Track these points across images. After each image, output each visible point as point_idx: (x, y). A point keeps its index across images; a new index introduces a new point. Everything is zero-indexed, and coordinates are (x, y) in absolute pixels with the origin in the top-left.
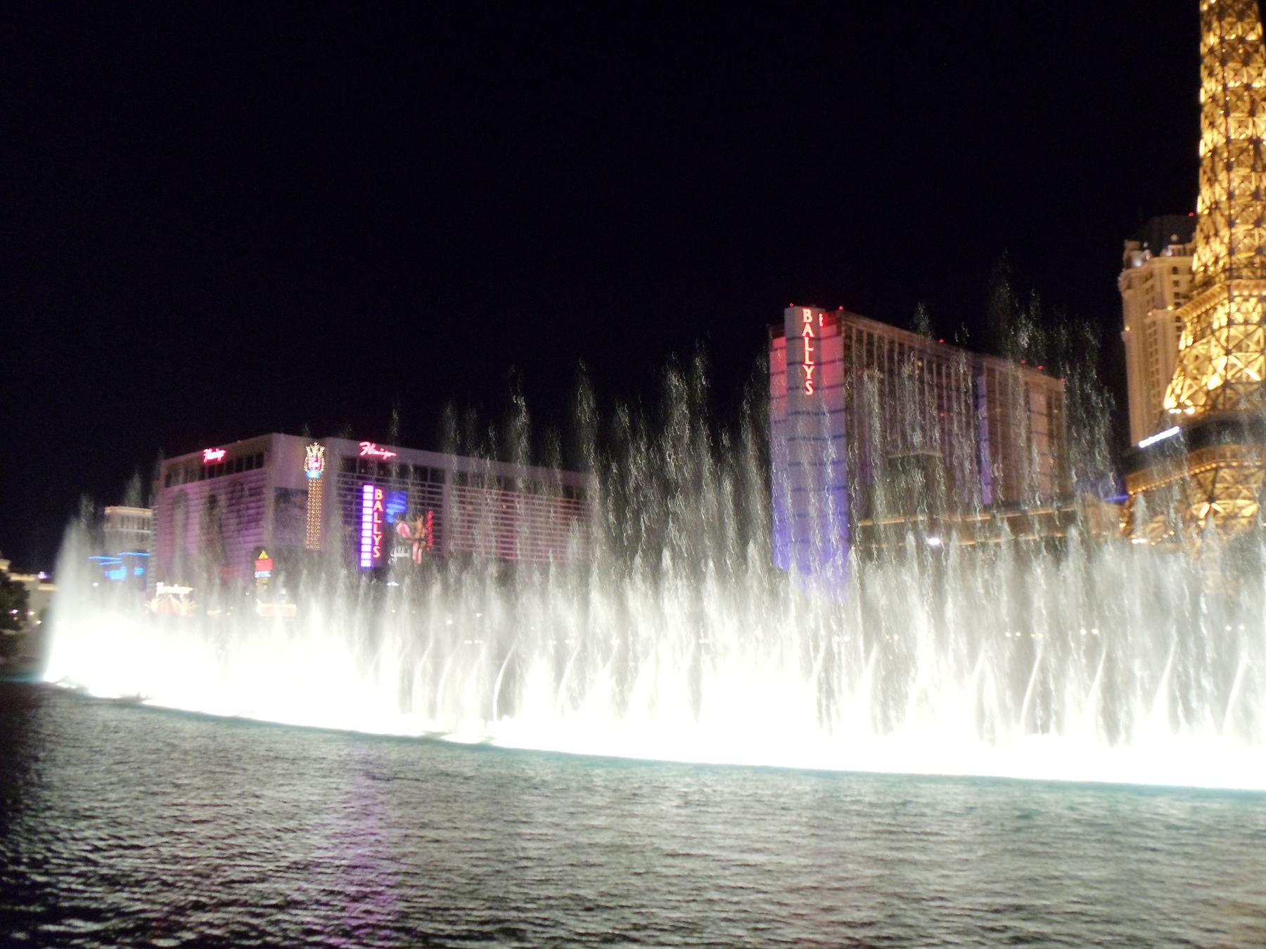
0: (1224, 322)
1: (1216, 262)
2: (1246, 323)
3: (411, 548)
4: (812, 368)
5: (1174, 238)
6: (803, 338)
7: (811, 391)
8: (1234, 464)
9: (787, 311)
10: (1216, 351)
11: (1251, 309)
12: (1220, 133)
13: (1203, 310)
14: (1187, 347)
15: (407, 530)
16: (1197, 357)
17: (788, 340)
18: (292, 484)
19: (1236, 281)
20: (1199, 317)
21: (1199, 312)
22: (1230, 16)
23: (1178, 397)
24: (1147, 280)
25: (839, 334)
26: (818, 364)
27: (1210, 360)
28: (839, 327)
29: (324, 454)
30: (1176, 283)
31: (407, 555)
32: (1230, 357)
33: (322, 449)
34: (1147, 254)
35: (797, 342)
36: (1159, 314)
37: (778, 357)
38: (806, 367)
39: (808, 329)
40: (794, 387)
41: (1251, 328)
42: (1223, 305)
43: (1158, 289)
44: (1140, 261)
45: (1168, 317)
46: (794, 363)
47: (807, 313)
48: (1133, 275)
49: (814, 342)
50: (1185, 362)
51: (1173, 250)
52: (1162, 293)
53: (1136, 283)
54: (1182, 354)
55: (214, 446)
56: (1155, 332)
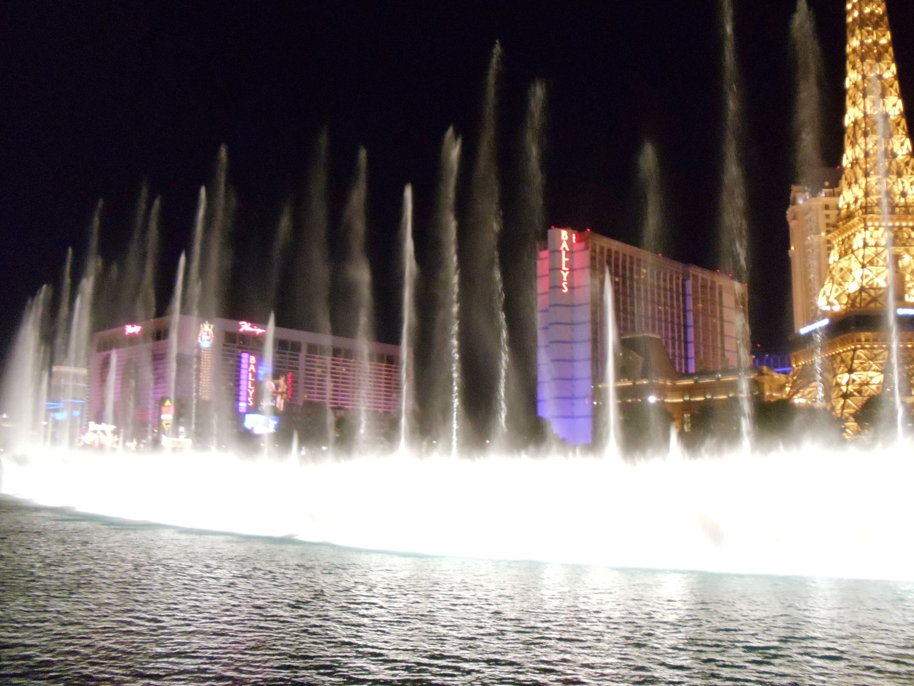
0: (861, 244)
1: (856, 201)
2: (877, 245)
4: (567, 273)
6: (560, 252)
7: (566, 290)
8: (867, 346)
10: (856, 266)
11: (880, 236)
12: (859, 109)
13: (847, 235)
14: (834, 262)
15: (273, 385)
16: (841, 270)
19: (870, 216)
20: (843, 240)
21: (843, 237)
23: (828, 298)
25: (587, 248)
27: (850, 271)
28: (587, 244)
30: (827, 216)
32: (865, 269)
33: (212, 326)
34: (807, 195)
35: (557, 254)
37: (542, 265)
38: (563, 272)
39: (565, 245)
41: (880, 249)
42: (860, 232)
45: (822, 240)
47: (564, 234)
48: (797, 210)
50: (833, 272)
51: (825, 193)
54: (831, 267)
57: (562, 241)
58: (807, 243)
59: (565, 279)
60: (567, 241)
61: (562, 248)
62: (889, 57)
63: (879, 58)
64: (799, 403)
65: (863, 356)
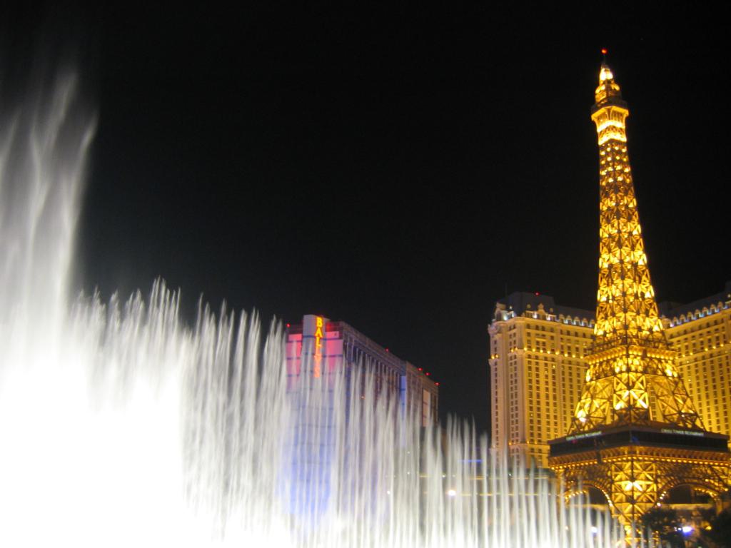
0: (624, 368)
1: (615, 331)
6: (315, 337)
8: (641, 458)
13: (605, 359)
17: (303, 337)
20: (601, 364)
21: (601, 360)
22: (620, 191)
24: (510, 329)
25: (340, 338)
28: (341, 334)
34: (512, 313)
35: (312, 339)
39: (319, 332)
44: (507, 317)
45: (524, 355)
47: (320, 321)
48: (502, 325)
49: (322, 341)
52: (521, 340)
53: (504, 330)
57: (317, 328)
60: (321, 329)
61: (316, 335)
62: (636, 219)
63: (630, 219)
64: (676, 508)
65: (639, 467)
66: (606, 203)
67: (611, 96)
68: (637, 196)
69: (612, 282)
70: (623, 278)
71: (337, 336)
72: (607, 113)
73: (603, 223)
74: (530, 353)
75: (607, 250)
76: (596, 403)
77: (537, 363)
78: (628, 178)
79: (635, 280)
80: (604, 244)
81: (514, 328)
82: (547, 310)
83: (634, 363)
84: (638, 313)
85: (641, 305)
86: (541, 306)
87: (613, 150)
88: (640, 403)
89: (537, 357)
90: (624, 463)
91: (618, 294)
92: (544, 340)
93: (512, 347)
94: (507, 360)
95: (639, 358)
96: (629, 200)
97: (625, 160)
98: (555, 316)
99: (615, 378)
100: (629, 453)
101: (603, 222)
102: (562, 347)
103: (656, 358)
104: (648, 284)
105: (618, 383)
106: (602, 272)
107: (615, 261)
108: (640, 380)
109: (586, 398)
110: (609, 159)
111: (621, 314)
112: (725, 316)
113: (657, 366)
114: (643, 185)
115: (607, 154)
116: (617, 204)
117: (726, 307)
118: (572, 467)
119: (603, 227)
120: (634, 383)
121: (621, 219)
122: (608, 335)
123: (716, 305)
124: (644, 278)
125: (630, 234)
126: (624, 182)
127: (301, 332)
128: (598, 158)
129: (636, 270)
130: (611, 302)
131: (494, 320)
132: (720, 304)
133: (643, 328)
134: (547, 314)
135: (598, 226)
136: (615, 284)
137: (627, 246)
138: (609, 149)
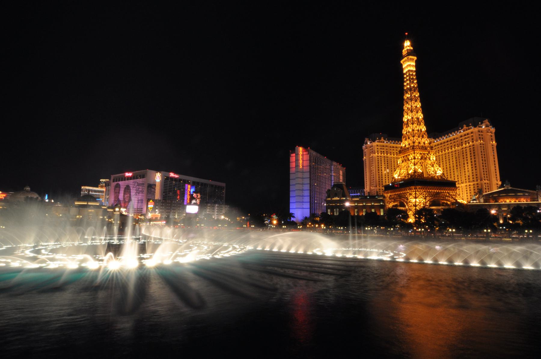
1: (409, 144)
2: (418, 159)
3: (197, 200)
5: (377, 138)
6: (299, 154)
7: (301, 167)
9: (296, 148)
13: (405, 155)
14: (400, 163)
15: (196, 195)
17: (296, 154)
18: (152, 183)
20: (404, 157)
21: (404, 155)
22: (412, 90)
24: (371, 147)
25: (308, 154)
26: (303, 161)
28: (308, 153)
29: (161, 175)
30: (378, 149)
31: (196, 202)
33: (160, 174)
36: (374, 155)
37: (293, 158)
40: (297, 166)
41: (419, 160)
43: (374, 149)
45: (376, 156)
46: (297, 160)
47: (301, 149)
48: (367, 146)
52: (375, 150)
53: (368, 148)
54: (399, 164)
55: (129, 172)
56: (373, 159)
58: (370, 156)
59: (301, 163)
62: (419, 101)
63: (416, 101)
65: (418, 194)
66: (406, 96)
67: (409, 52)
68: (419, 92)
69: (409, 126)
70: (413, 124)
71: (307, 154)
72: (407, 59)
73: (405, 104)
74: (378, 155)
75: (406, 114)
76: (402, 171)
77: (381, 159)
78: (415, 85)
79: (418, 125)
80: (405, 112)
81: (372, 146)
82: (385, 139)
83: (417, 156)
84: (419, 137)
85: (420, 134)
86: (382, 138)
87: (409, 74)
88: (420, 171)
89: (381, 157)
90: (413, 192)
91: (411, 130)
92: (384, 150)
93: (372, 153)
94: (370, 158)
95: (419, 154)
96: (416, 93)
97: (414, 78)
98: (388, 141)
99: (409, 162)
100: (414, 189)
101: (405, 103)
102: (391, 152)
103: (426, 153)
104: (423, 126)
105: (410, 164)
106: (405, 123)
107: (410, 118)
108: (419, 162)
109: (398, 170)
110: (408, 78)
111: (412, 138)
112: (458, 136)
113: (427, 157)
114: (421, 88)
115: (407, 76)
116: (411, 96)
117: (459, 133)
118: (393, 194)
119: (405, 105)
120: (417, 163)
121: (413, 101)
122: (407, 146)
123: (454, 132)
124: (422, 123)
125: (416, 107)
126: (414, 87)
127: (295, 153)
128: (404, 78)
129: (418, 121)
130: (408, 133)
131: (364, 144)
132: (456, 132)
133: (421, 142)
134: (384, 141)
135: (403, 105)
136: (410, 127)
137: (415, 112)
138: (408, 74)
